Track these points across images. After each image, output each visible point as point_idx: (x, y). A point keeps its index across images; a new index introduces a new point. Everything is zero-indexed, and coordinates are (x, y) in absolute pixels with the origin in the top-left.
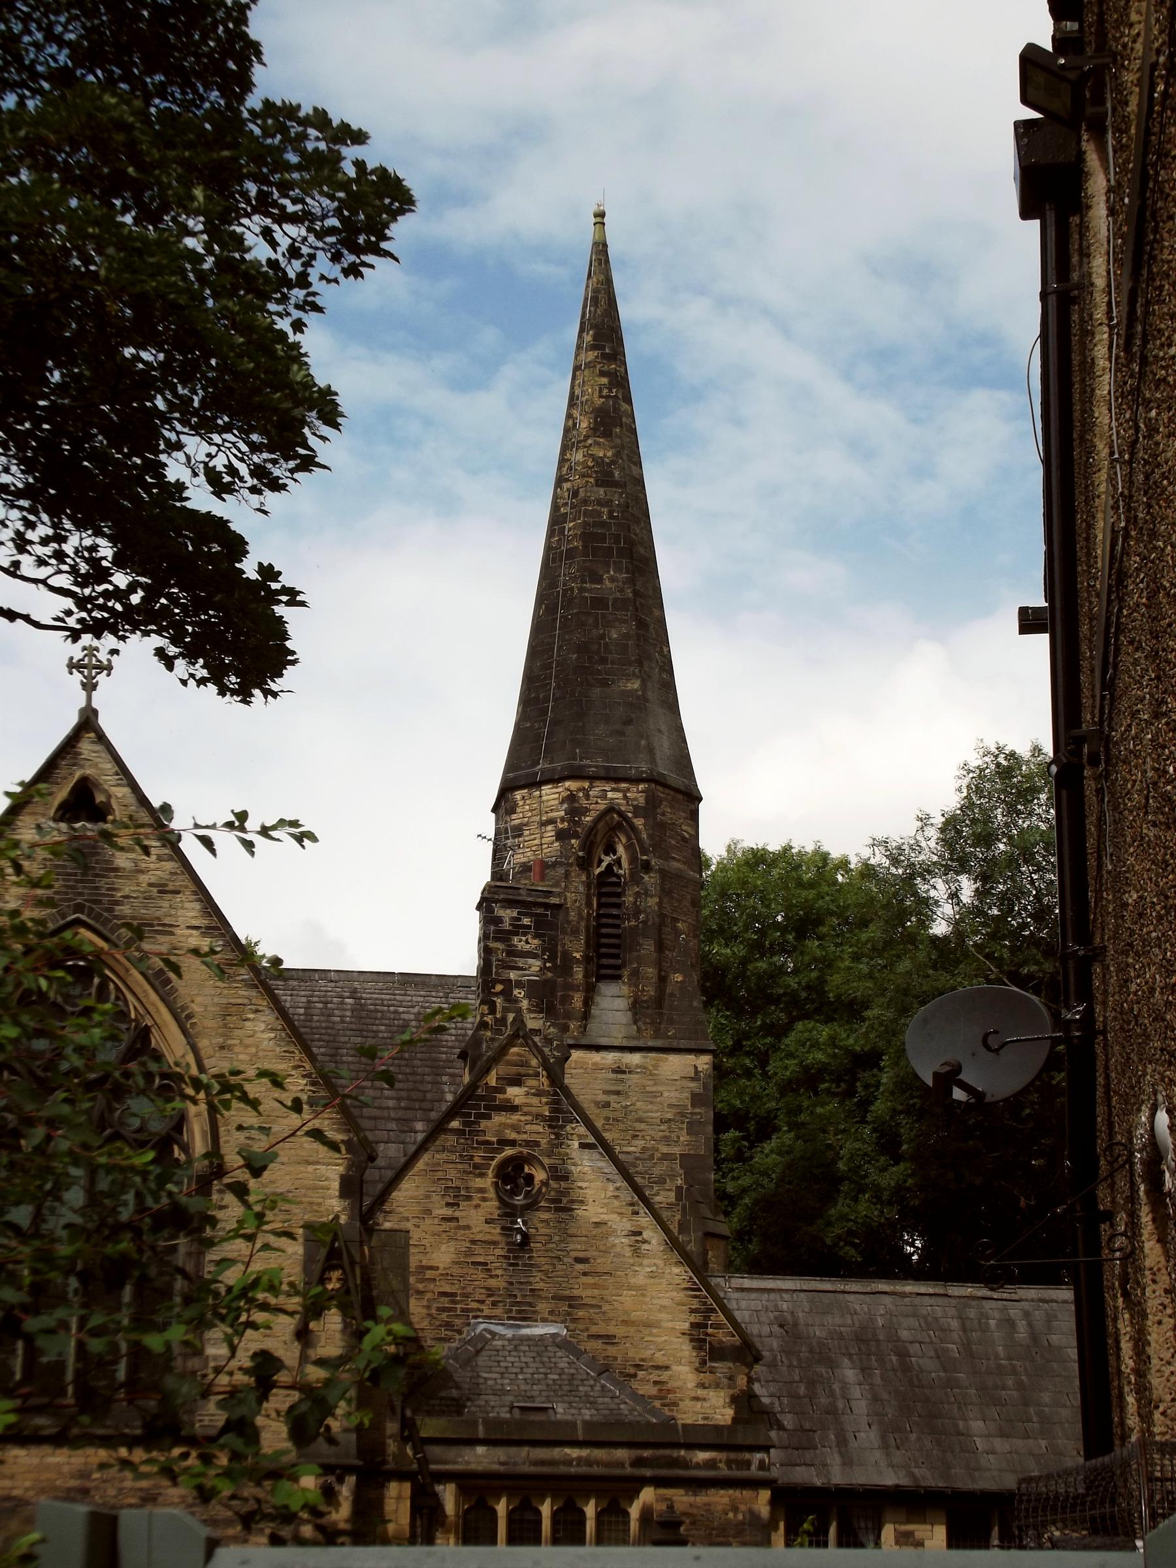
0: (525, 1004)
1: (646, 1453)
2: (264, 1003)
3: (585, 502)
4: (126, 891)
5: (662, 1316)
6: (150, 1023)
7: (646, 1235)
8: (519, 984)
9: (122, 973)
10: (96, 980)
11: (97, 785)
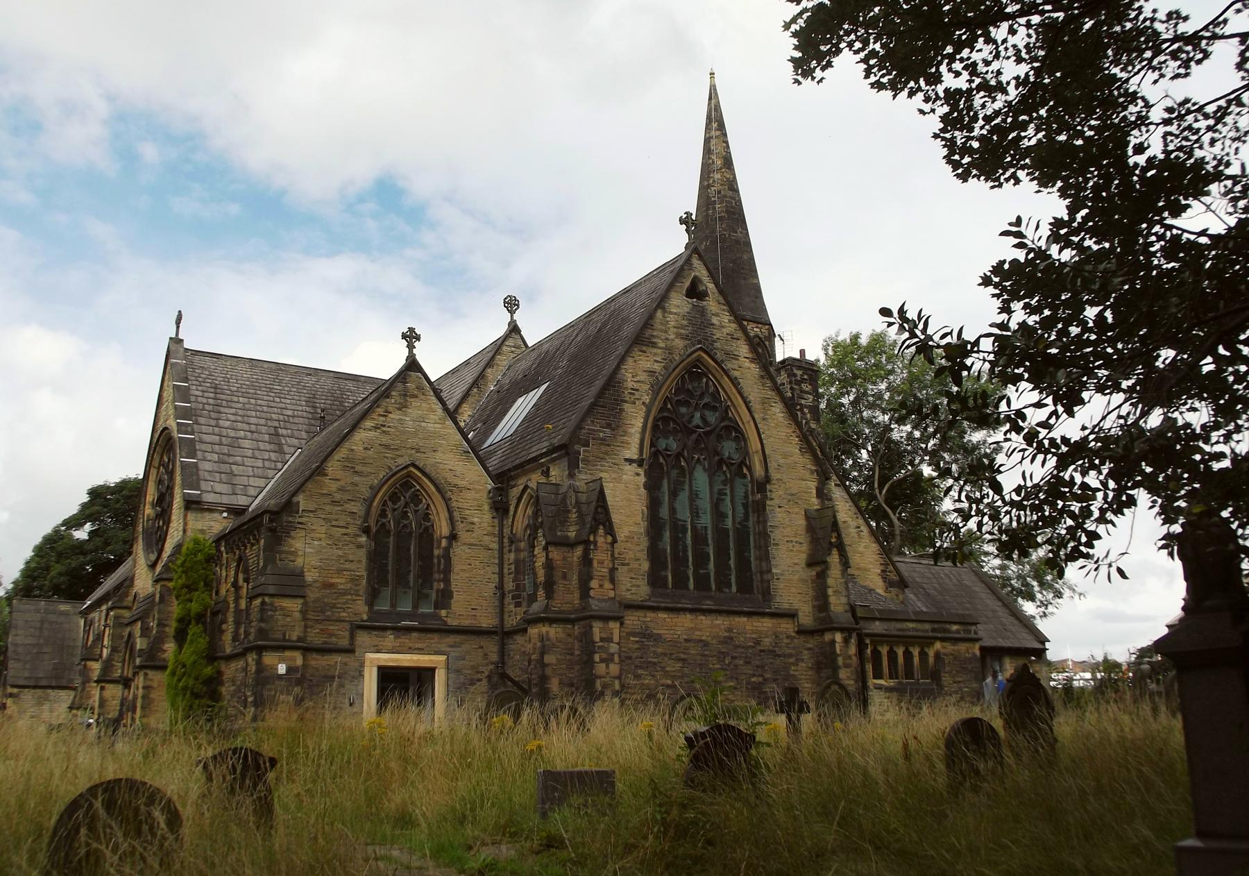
3: (725, 196)
4: (718, 336)
8: (806, 407)
11: (701, 281)
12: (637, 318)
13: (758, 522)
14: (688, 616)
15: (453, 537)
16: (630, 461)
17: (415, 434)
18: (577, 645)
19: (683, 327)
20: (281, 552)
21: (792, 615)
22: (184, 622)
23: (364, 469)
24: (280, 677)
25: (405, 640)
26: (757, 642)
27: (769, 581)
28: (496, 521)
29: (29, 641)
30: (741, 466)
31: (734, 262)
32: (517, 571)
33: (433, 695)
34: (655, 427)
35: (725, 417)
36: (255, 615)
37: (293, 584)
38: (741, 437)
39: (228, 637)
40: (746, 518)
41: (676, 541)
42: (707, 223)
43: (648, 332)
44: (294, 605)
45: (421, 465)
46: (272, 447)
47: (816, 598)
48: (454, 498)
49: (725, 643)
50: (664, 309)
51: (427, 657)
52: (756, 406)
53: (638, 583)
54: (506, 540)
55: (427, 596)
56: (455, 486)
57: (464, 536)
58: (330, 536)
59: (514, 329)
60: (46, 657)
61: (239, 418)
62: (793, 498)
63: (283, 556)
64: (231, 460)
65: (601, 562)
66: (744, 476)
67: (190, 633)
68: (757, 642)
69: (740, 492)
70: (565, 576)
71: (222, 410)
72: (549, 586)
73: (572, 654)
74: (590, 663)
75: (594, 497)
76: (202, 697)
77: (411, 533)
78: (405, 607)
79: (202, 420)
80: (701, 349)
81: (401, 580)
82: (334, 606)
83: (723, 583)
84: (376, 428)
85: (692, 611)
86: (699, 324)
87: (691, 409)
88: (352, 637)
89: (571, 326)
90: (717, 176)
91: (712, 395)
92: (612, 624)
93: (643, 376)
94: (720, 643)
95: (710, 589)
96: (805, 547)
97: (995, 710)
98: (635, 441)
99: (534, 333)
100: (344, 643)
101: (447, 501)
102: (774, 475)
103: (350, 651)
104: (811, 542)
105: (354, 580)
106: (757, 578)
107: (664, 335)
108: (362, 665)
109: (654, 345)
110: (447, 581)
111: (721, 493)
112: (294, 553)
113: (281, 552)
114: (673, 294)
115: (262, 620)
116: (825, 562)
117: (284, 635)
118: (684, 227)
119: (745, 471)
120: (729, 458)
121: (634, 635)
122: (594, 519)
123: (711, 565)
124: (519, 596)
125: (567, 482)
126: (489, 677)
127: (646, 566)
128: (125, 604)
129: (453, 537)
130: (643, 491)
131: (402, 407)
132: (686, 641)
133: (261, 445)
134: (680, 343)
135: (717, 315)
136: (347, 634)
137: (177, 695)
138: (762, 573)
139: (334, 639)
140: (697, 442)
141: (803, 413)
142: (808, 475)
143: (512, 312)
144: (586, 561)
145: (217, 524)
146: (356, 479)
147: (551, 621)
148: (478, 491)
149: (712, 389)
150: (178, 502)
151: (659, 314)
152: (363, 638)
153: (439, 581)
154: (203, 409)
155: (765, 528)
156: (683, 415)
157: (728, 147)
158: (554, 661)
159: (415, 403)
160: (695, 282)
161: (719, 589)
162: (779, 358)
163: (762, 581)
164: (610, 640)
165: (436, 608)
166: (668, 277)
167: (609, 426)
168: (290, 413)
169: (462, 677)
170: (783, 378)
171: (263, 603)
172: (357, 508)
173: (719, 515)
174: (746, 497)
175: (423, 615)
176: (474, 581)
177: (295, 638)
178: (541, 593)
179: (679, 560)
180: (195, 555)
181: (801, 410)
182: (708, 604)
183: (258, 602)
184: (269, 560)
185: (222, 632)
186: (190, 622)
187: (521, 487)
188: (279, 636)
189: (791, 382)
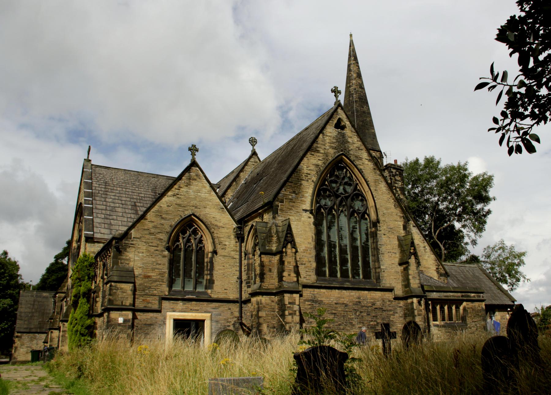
0: (399, 192)
1: (463, 294)
2: (383, 180)
4: (351, 148)
5: (431, 266)
6: (358, 182)
7: (427, 247)
8: (398, 188)
9: (352, 169)
10: (345, 170)
11: (342, 120)
12: (310, 140)
13: (373, 242)
14: (337, 291)
15: (215, 252)
16: (306, 211)
17: (195, 199)
18: (277, 307)
19: (333, 143)
20: (121, 259)
21: (391, 290)
22: (77, 297)
23: (167, 216)
24: (120, 325)
25: (189, 305)
26: (373, 304)
27: (379, 272)
28: (238, 244)
29: (28, 310)
30: (363, 215)
31: (363, 121)
32: (248, 269)
33: (204, 333)
34: (319, 195)
35: (355, 189)
36: (107, 293)
37: (129, 276)
38: (364, 199)
39: (99, 305)
40: (367, 240)
41: (330, 252)
42: (349, 104)
43: (315, 145)
44: (128, 287)
45: (198, 215)
46: (133, 211)
47: (403, 281)
48: (215, 232)
49: (356, 304)
50: (323, 133)
51: (200, 314)
52: (371, 184)
53: (310, 274)
54: (243, 254)
55: (201, 283)
56: (216, 225)
57: (220, 251)
58: (149, 251)
59: (254, 153)
60: (36, 318)
61: (117, 198)
62: (391, 230)
63: (123, 261)
64: (111, 218)
65: (289, 263)
66: (366, 219)
67: (80, 302)
68: (373, 304)
69: (364, 227)
70: (270, 270)
71: (108, 193)
72: (262, 276)
73: (274, 311)
74: (283, 316)
75: (286, 228)
76: (85, 336)
77: (192, 250)
78: (189, 288)
79: (97, 198)
80: (343, 154)
81: (187, 274)
82: (150, 287)
83: (356, 273)
84: (174, 195)
85: (339, 288)
86: (342, 141)
87: (338, 185)
88: (160, 304)
89: (280, 149)
90: (354, 82)
91: (349, 177)
92: (295, 295)
93: (312, 167)
94: (354, 304)
95: (348, 277)
96: (398, 255)
99: (263, 154)
100: (156, 307)
101: (211, 233)
102: (381, 218)
103: (159, 311)
104: (401, 253)
105: (162, 274)
106: (373, 271)
107: (323, 147)
108: (165, 319)
109: (318, 151)
110: (211, 275)
111: (354, 228)
112: (129, 260)
113: (121, 259)
114: (328, 126)
115: (110, 295)
116: (407, 263)
117: (122, 302)
118: (334, 94)
119: (366, 216)
120: (358, 210)
121: (308, 301)
122: (285, 240)
123: (349, 265)
124: (249, 282)
125: (272, 221)
126: (234, 324)
127: (314, 265)
128: (63, 291)
129: (215, 252)
130: (313, 227)
131: (188, 185)
132: (336, 304)
133: (127, 211)
134: (332, 151)
135: (351, 137)
136: (157, 302)
137: (72, 334)
138: (375, 268)
139: (150, 305)
140: (341, 202)
141: (396, 191)
142: (399, 219)
143: (253, 146)
144: (281, 262)
145: (98, 247)
146: (163, 221)
147: (263, 294)
148: (228, 228)
149: (348, 175)
150: (83, 239)
151: (321, 136)
152: (165, 304)
153: (207, 275)
154: (99, 193)
155: (377, 245)
156: (334, 188)
157: (359, 68)
158: (265, 315)
159: (195, 183)
160: (340, 120)
161: (353, 277)
162: (385, 164)
163: (376, 273)
164: (293, 303)
165: (206, 288)
166: (326, 118)
167: (294, 192)
168: (143, 195)
169: (219, 324)
170: (386, 173)
171: (111, 286)
172: (164, 237)
173: (353, 239)
174: (367, 230)
175: (199, 292)
176: (226, 274)
177: (128, 304)
178: (258, 279)
179: (332, 262)
180: (84, 263)
181: (396, 189)
182: (347, 285)
183: (108, 285)
184: (115, 263)
185: (97, 302)
186: (80, 297)
187: (250, 226)
188: (119, 303)
189: (390, 176)
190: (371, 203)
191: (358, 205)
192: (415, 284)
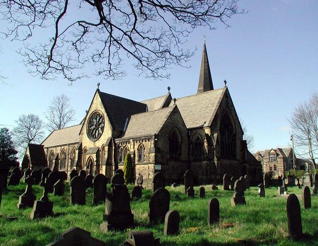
21: (239, 160)
78: (174, 156)
97: (197, 187)
98: (219, 125)
129: (182, 142)
190: (234, 127)
191: (230, 128)
192: (246, 159)
